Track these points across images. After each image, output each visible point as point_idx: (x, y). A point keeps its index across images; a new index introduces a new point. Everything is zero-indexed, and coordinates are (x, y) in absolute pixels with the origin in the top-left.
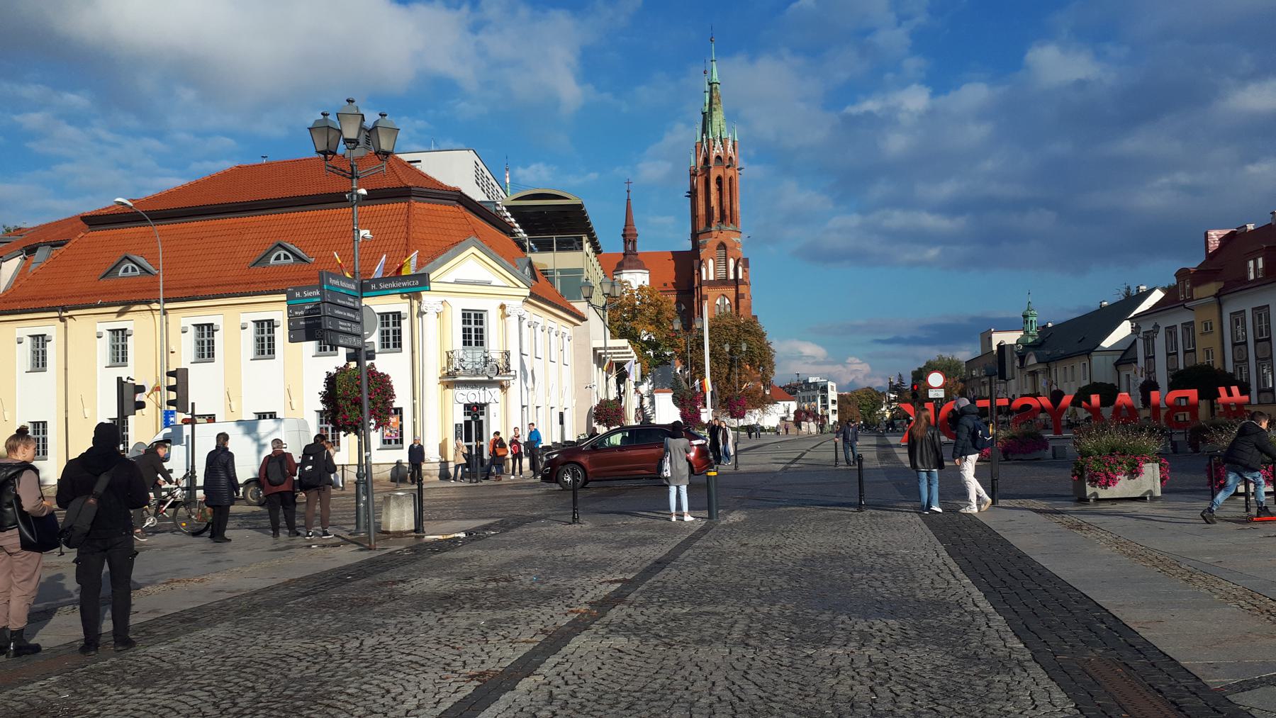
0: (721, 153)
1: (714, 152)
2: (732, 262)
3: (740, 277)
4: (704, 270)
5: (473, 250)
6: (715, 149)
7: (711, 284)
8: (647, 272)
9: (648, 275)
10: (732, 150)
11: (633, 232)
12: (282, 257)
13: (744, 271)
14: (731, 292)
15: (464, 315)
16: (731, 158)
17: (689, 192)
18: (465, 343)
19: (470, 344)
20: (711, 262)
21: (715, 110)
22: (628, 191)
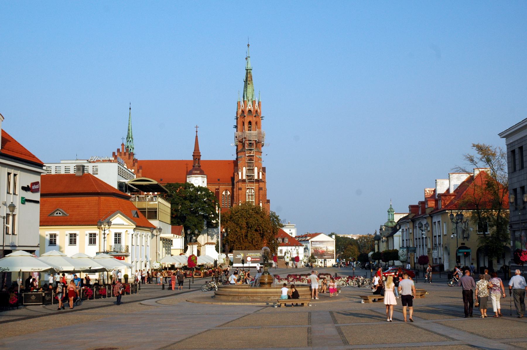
0: (251, 108)
1: (248, 108)
2: (256, 169)
3: (261, 178)
4: (240, 173)
5: (119, 214)
6: (248, 106)
8: (206, 176)
9: (206, 178)
10: (258, 107)
11: (199, 154)
12: (58, 213)
13: (263, 174)
14: (255, 186)
15: (115, 234)
16: (257, 111)
17: (235, 126)
18: (115, 243)
19: (116, 243)
21: (249, 84)
22: (197, 132)
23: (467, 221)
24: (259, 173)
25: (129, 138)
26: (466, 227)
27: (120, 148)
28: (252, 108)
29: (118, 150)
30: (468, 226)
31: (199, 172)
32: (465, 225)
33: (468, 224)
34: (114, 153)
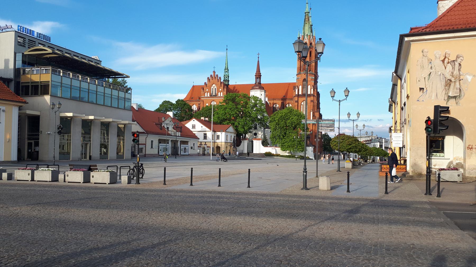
2: (309, 86)
4: (297, 90)
7: (298, 96)
8: (264, 90)
20: (300, 87)
21: (306, 23)
22: (258, 58)
23: (459, 60)
24: (311, 89)
25: (226, 70)
26: (456, 72)
27: (212, 74)
28: (307, 41)
29: (211, 76)
30: (459, 70)
31: (258, 87)
32: (453, 68)
33: (460, 65)
34: (208, 78)
